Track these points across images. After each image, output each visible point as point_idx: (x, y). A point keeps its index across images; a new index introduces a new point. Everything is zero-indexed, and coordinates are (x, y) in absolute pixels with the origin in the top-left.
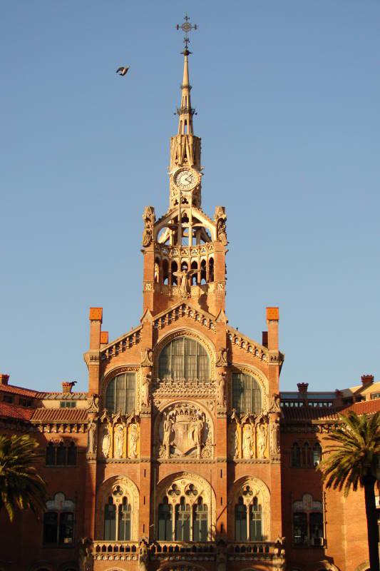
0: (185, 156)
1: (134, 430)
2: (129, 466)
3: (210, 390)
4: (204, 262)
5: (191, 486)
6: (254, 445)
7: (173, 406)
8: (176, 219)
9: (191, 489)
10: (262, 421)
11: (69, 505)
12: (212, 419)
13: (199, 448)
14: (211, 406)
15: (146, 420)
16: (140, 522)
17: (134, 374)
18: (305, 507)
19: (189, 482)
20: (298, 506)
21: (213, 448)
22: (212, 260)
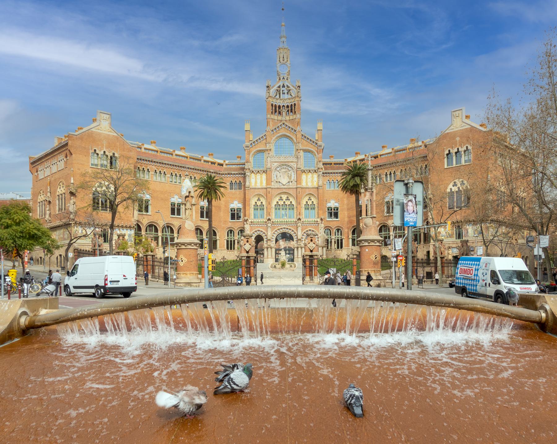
0: (283, 58)
1: (264, 176)
4: (292, 105)
5: (288, 197)
6: (312, 181)
7: (280, 166)
8: (279, 87)
9: (288, 199)
10: (315, 171)
11: (240, 206)
19: (287, 196)
20: (329, 205)
22: (295, 104)
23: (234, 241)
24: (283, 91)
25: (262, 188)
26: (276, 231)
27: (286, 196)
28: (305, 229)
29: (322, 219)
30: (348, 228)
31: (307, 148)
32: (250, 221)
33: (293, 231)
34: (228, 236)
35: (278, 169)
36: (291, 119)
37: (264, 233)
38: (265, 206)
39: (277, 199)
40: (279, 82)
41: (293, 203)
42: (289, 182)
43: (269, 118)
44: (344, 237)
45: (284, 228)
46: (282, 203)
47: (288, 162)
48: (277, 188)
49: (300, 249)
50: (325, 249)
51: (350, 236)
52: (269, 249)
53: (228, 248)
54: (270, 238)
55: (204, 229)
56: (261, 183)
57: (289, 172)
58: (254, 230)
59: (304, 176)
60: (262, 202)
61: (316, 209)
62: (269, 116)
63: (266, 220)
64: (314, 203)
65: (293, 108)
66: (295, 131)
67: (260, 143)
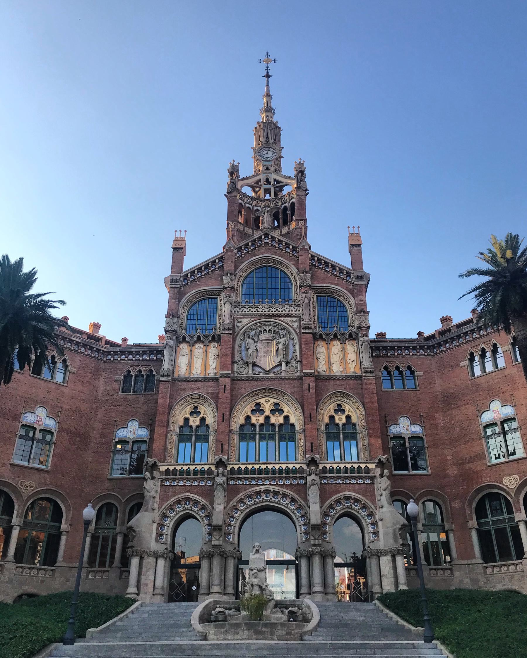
0: (267, 138)
1: (213, 349)
2: (206, 383)
4: (285, 208)
5: (276, 404)
6: (344, 361)
9: (277, 409)
10: (350, 335)
11: (143, 433)
12: (298, 336)
13: (284, 365)
14: (296, 324)
15: (226, 339)
16: (217, 440)
17: (217, 298)
18: (402, 431)
19: (273, 401)
20: (394, 430)
21: (299, 364)
25: (206, 380)
26: (241, 501)
27: (273, 401)
29: (380, 464)
31: (324, 285)
32: (163, 468)
33: (293, 500)
35: (252, 333)
36: (283, 233)
37: (203, 508)
38: (211, 429)
39: (248, 410)
40: (258, 175)
41: (292, 420)
42: (280, 365)
45: (267, 492)
47: (280, 316)
48: (248, 379)
49: (317, 561)
50: (401, 562)
51: (473, 523)
52: (216, 562)
53: (91, 562)
54: (220, 523)
55: (19, 494)
56: (205, 364)
57: (280, 340)
59: (321, 349)
60: (203, 419)
61: (359, 437)
62: (232, 225)
63: (213, 468)
64: (354, 420)
65: (289, 212)
66: (294, 249)
67: (207, 276)
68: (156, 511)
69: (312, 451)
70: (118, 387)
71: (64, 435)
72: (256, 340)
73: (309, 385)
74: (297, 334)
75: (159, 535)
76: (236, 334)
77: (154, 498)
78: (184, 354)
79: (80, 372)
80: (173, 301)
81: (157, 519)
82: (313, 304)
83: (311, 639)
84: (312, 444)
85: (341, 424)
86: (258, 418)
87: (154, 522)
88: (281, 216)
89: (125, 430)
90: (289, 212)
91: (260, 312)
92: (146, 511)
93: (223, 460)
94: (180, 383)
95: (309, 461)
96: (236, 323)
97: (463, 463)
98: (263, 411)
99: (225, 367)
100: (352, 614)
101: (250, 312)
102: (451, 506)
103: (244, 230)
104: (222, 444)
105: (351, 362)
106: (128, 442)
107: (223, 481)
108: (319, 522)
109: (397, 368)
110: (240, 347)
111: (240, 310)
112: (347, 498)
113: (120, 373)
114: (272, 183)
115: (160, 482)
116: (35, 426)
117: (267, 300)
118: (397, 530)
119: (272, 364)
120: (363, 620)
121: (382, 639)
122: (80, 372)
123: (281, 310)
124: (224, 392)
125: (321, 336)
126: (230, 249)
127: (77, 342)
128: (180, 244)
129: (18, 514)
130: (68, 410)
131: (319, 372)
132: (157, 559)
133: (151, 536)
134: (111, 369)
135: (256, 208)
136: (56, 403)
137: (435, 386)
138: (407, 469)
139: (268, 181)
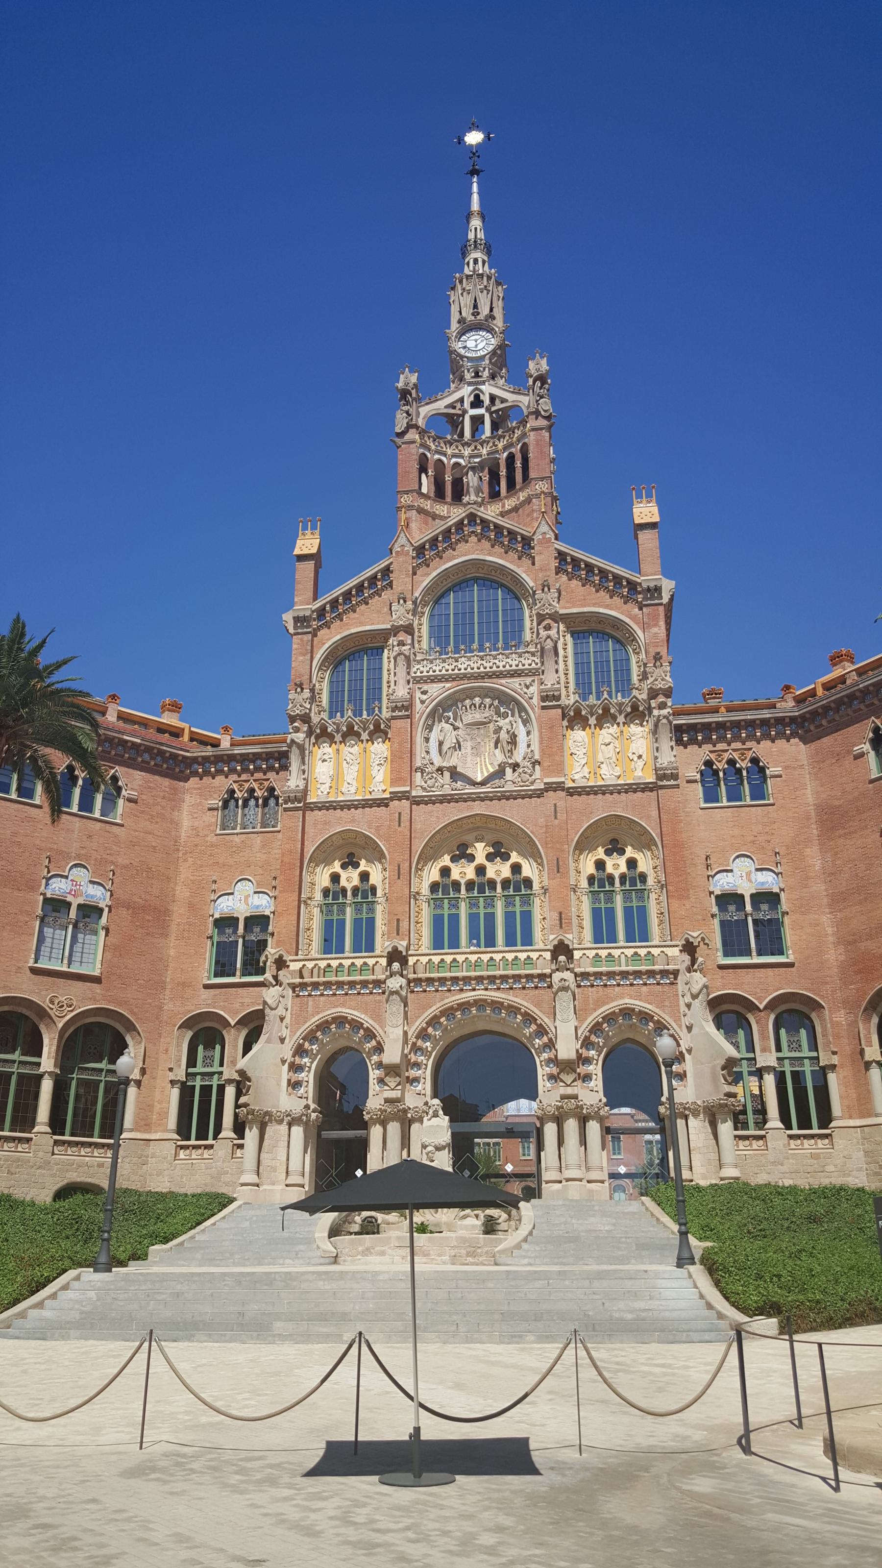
0: (475, 306)
3: (527, 662)
4: (511, 458)
10: (635, 708)
13: (509, 771)
23: (221, 1089)
24: (473, 418)
28: (599, 1003)
30: (849, 1005)
32: (295, 966)
34: (192, 1061)
36: (507, 507)
43: (410, 508)
44: (835, 1060)
45: (480, 1004)
46: (471, 874)
56: (365, 776)
58: (315, 1020)
65: (518, 464)
67: (363, 607)
68: (287, 1041)
69: (561, 927)
70: (213, 820)
71: (123, 912)
72: (458, 724)
73: (555, 805)
74: (532, 709)
75: (295, 1085)
76: (417, 716)
77: (282, 1019)
78: (325, 757)
79: (144, 797)
80: (301, 658)
81: (288, 1055)
82: (565, 649)
83: (510, 1262)
84: (560, 914)
85: (617, 875)
86: (464, 870)
87: (283, 1062)
88: (503, 472)
89: (231, 897)
90: (518, 464)
91: (463, 671)
92: (268, 1041)
93: (400, 949)
94: (320, 813)
95: (555, 947)
96: (418, 695)
97: (855, 941)
98: (471, 858)
99: (400, 779)
100: (592, 1220)
101: (444, 672)
102: (831, 1019)
103: (432, 507)
104: (398, 920)
105: (636, 759)
106: (237, 919)
107: (401, 987)
108: (573, 1056)
109: (732, 762)
110: (427, 740)
111: (425, 669)
112: (627, 1012)
113: (216, 796)
114: (487, 401)
115: (290, 991)
116: (68, 899)
117: (475, 646)
118: (719, 1068)
119: (487, 769)
120: (609, 1231)
121: (633, 1261)
122: (144, 797)
123: (501, 664)
124: (399, 825)
125: (578, 712)
126: (403, 550)
127: (133, 743)
128: (310, 547)
129: (49, 1053)
130: (125, 867)
131: (573, 781)
132: (290, 1125)
133: (279, 1085)
134: (199, 789)
135: (454, 460)
136: (104, 856)
137: (804, 794)
138: (749, 953)
139: (477, 402)
